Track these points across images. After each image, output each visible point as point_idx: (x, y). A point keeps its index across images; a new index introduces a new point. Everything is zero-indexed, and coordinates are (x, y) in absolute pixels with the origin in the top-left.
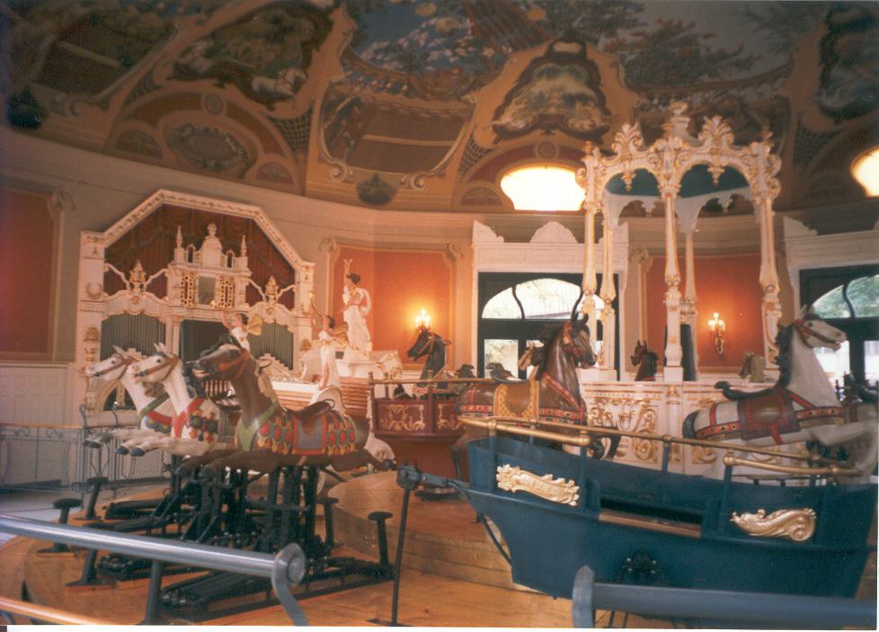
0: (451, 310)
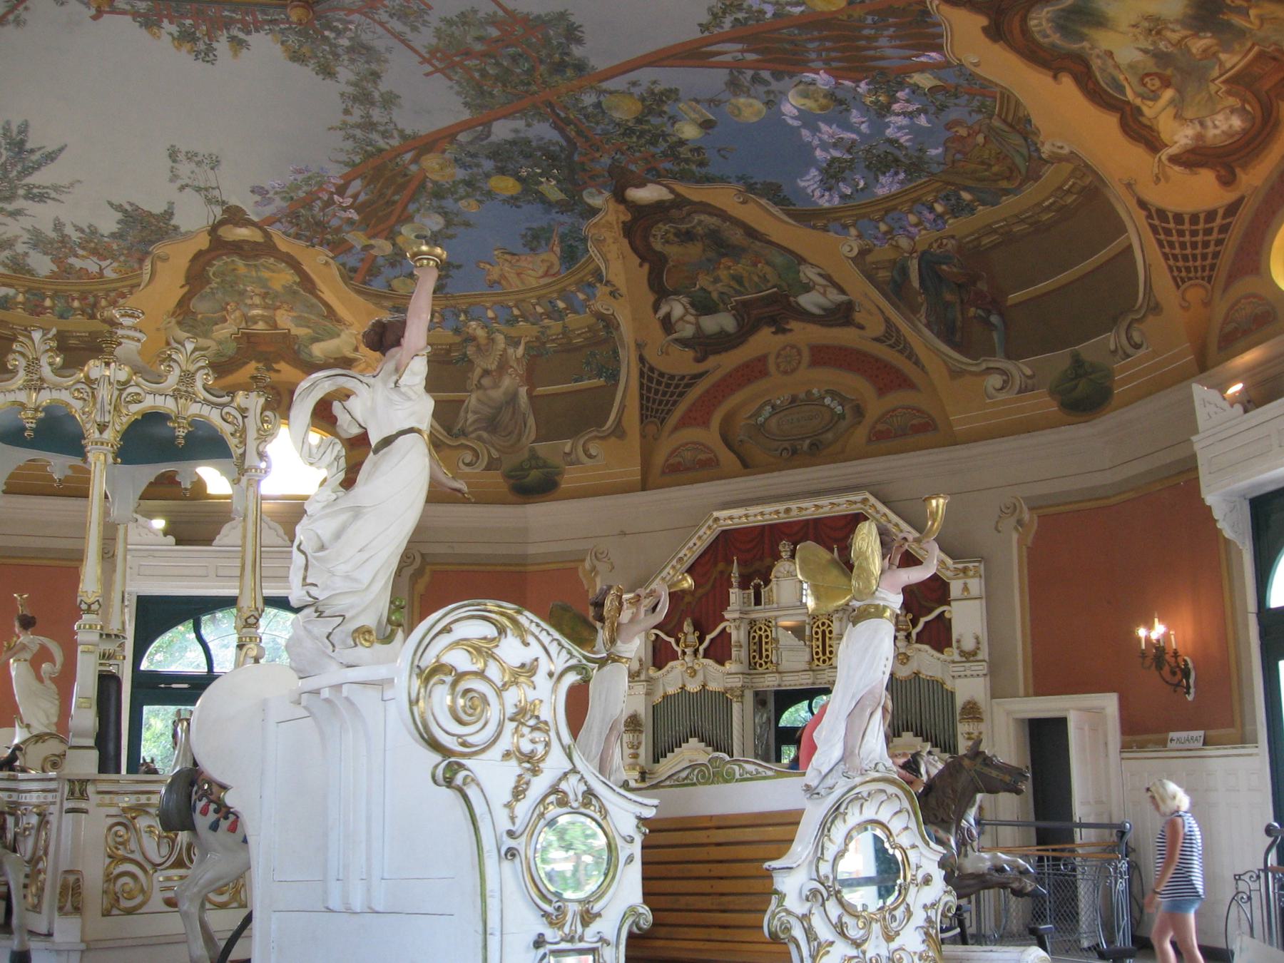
0: (1227, 595)
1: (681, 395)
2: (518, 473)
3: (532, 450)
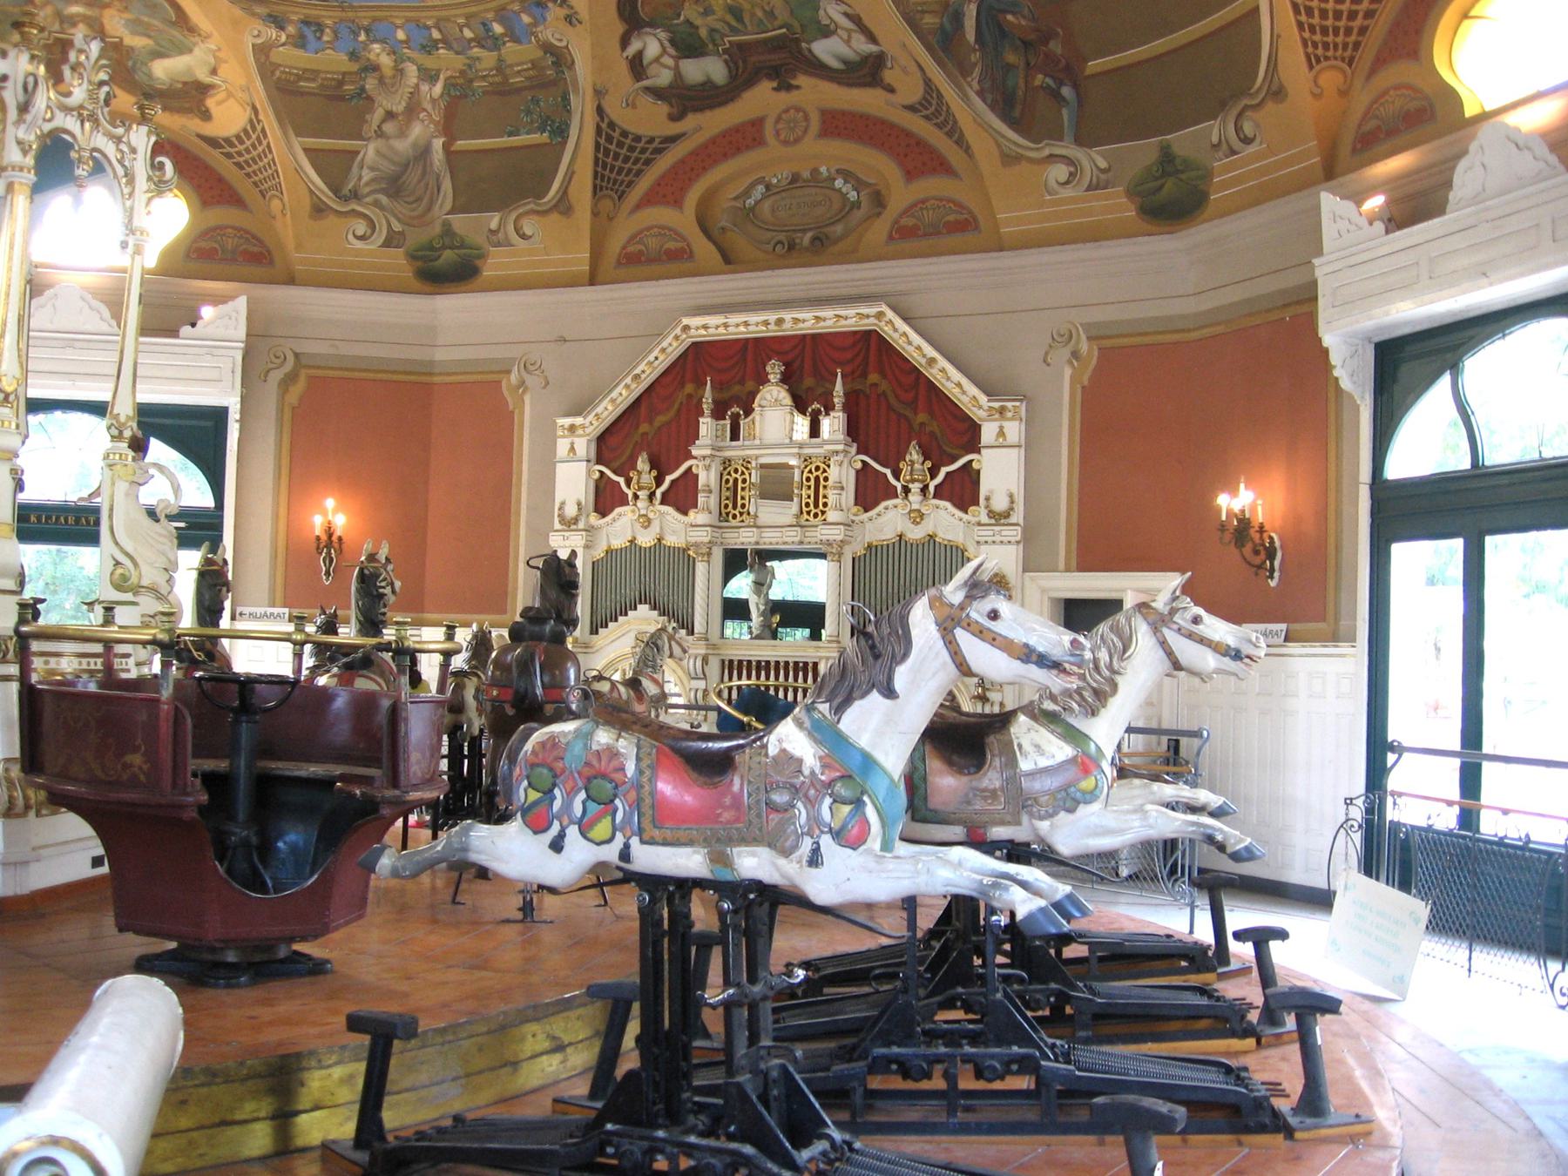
1: (648, 162)
2: (428, 253)
3: (447, 227)
